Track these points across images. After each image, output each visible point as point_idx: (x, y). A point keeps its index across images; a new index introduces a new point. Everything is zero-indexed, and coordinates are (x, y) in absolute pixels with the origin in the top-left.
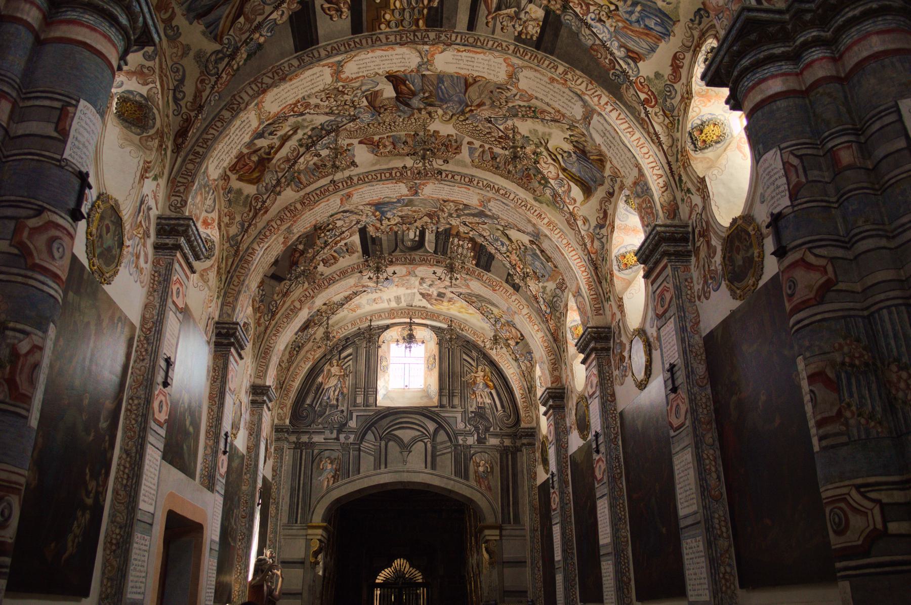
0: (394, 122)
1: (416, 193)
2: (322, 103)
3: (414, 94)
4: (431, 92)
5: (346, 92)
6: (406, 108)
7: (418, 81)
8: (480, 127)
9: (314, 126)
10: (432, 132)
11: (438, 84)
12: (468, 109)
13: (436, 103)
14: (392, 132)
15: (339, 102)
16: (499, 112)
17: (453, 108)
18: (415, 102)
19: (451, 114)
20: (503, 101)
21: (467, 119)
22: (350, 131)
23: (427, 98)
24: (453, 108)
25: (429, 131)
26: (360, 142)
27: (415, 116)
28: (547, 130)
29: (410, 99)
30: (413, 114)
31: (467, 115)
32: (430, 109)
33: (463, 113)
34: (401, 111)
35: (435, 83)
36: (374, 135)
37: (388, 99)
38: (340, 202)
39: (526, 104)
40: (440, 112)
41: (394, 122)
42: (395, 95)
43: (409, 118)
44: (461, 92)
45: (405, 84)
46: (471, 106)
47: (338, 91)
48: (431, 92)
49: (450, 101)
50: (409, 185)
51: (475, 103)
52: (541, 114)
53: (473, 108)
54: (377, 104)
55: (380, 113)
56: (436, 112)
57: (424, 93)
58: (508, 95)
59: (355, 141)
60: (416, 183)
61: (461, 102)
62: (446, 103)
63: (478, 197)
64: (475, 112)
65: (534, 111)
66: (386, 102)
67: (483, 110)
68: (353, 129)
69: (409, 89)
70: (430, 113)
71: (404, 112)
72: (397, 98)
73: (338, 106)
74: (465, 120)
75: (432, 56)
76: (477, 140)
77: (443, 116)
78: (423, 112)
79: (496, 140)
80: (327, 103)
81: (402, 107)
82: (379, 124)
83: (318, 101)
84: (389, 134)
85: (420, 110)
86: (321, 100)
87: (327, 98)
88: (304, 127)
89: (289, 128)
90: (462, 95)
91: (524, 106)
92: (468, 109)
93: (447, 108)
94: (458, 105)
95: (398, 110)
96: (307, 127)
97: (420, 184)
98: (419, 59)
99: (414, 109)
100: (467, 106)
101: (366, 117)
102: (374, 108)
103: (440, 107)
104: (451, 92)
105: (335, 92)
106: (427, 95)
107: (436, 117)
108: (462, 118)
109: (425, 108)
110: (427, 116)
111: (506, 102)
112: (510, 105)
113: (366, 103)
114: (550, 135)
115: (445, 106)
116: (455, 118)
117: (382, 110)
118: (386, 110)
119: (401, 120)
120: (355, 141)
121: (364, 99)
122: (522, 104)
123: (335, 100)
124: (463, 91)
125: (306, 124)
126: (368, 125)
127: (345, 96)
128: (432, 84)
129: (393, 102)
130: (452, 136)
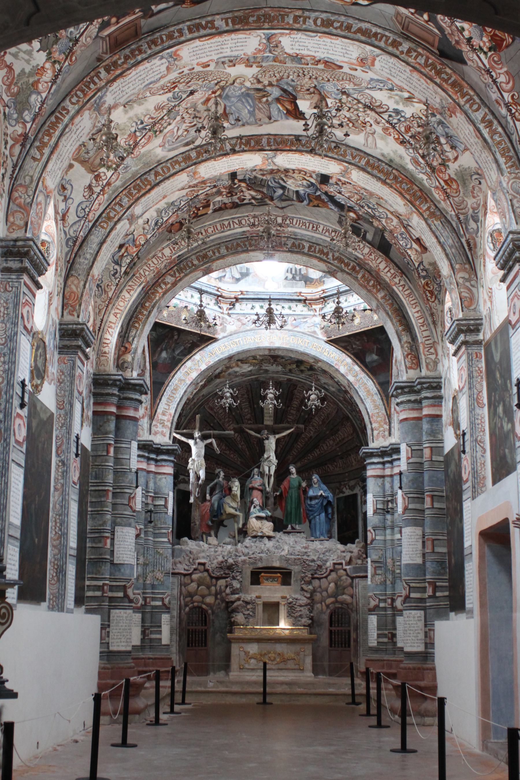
0: (299, 76)
1: (269, 39)
2: (372, 122)
3: (278, 100)
4: (260, 102)
5: (346, 120)
6: (286, 87)
7: (274, 113)
8: (200, 82)
9: (389, 92)
10: (254, 66)
11: (254, 110)
12: (218, 93)
13: (252, 92)
14: (302, 68)
15: (355, 112)
16: (186, 105)
17: (234, 90)
18: (276, 92)
19: (235, 84)
20: (186, 116)
21: (216, 84)
22: (350, 81)
23: (264, 96)
24: (234, 90)
25: (257, 67)
26: (341, 67)
27: (275, 79)
28: (131, 113)
29: (281, 96)
30: (278, 81)
31: (217, 87)
32: (260, 86)
33: (223, 88)
34: (291, 86)
35: (257, 111)
36: (323, 70)
37: (305, 99)
38: (377, 62)
39: (166, 131)
40: (248, 84)
41: (299, 76)
42: (298, 102)
43: (282, 78)
44: (230, 107)
45: (287, 110)
46: (215, 97)
47: (353, 124)
48: (260, 102)
49: (239, 96)
50: (279, 50)
51: (212, 101)
52: (150, 136)
53: (213, 95)
54: (316, 97)
55: (315, 87)
56: (252, 84)
57: (267, 100)
58: (185, 125)
59: (346, 69)
60: (270, 52)
61: (228, 97)
62: (243, 93)
63: (183, 62)
64: (210, 93)
65: (156, 131)
66: (308, 97)
67: (202, 98)
68: (347, 82)
69: (283, 106)
70: (259, 82)
71: (287, 84)
72: (295, 98)
73: (357, 110)
74: (218, 82)
75: (264, 163)
76: (199, 72)
77: (244, 81)
78: (266, 83)
79: (179, 82)
80: (367, 119)
81: (290, 89)
82: (316, 78)
83: (374, 126)
84: (305, 66)
85: (270, 84)
86: (371, 125)
87: (365, 124)
88: (400, 97)
89: (415, 104)
90: (228, 104)
91: (166, 128)
92: (218, 93)
93: (241, 89)
94: (230, 94)
95: (295, 88)
96: (397, 95)
97: (264, 51)
98: (275, 160)
99: (278, 86)
100: (220, 96)
101: (330, 88)
102: (320, 94)
103: (248, 89)
104: (239, 105)
105: (356, 125)
106: (264, 99)
107: (251, 79)
108: (222, 84)
109: (265, 86)
110: (261, 80)
111: (183, 118)
112: (179, 118)
113: (329, 101)
114: (126, 112)
115: (243, 90)
116: (231, 81)
117: (312, 90)
118: (308, 90)
119: (291, 77)
120: (346, 69)
121: (330, 105)
122: (169, 128)
123: (359, 117)
124: (228, 108)
125: (397, 97)
126: (329, 80)
127: (348, 116)
128: (259, 109)
129: (300, 95)
130: (229, 66)
